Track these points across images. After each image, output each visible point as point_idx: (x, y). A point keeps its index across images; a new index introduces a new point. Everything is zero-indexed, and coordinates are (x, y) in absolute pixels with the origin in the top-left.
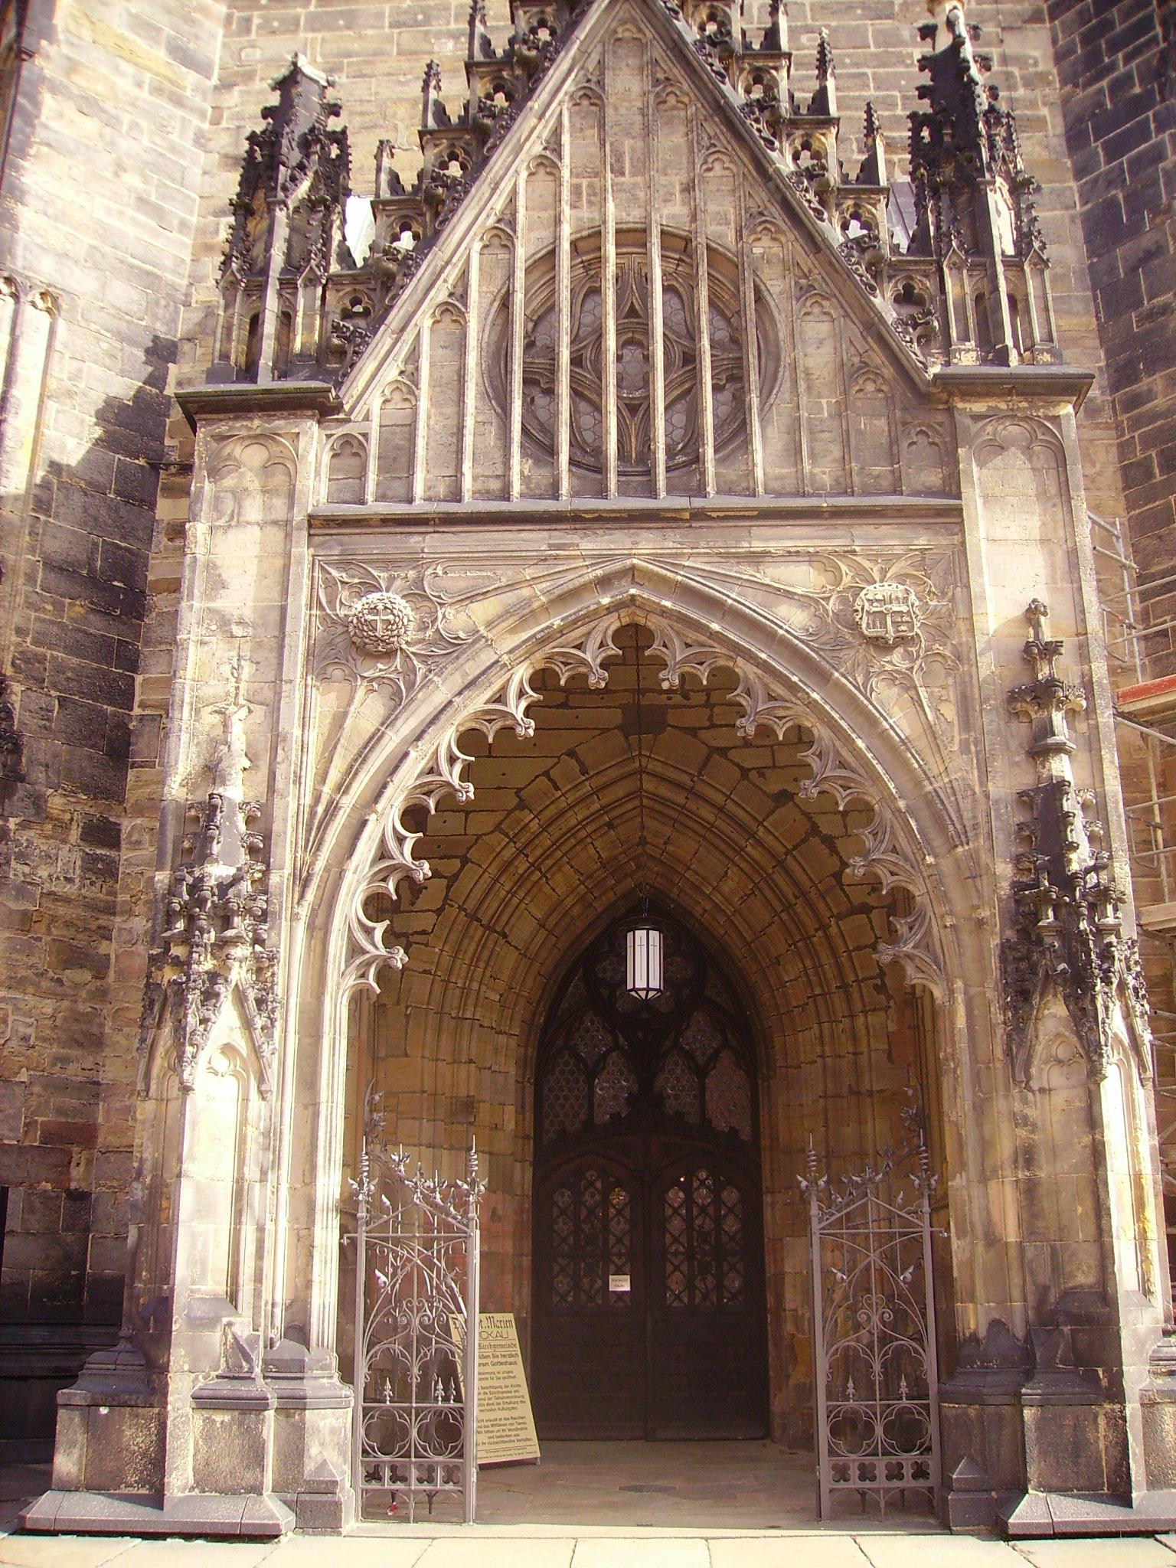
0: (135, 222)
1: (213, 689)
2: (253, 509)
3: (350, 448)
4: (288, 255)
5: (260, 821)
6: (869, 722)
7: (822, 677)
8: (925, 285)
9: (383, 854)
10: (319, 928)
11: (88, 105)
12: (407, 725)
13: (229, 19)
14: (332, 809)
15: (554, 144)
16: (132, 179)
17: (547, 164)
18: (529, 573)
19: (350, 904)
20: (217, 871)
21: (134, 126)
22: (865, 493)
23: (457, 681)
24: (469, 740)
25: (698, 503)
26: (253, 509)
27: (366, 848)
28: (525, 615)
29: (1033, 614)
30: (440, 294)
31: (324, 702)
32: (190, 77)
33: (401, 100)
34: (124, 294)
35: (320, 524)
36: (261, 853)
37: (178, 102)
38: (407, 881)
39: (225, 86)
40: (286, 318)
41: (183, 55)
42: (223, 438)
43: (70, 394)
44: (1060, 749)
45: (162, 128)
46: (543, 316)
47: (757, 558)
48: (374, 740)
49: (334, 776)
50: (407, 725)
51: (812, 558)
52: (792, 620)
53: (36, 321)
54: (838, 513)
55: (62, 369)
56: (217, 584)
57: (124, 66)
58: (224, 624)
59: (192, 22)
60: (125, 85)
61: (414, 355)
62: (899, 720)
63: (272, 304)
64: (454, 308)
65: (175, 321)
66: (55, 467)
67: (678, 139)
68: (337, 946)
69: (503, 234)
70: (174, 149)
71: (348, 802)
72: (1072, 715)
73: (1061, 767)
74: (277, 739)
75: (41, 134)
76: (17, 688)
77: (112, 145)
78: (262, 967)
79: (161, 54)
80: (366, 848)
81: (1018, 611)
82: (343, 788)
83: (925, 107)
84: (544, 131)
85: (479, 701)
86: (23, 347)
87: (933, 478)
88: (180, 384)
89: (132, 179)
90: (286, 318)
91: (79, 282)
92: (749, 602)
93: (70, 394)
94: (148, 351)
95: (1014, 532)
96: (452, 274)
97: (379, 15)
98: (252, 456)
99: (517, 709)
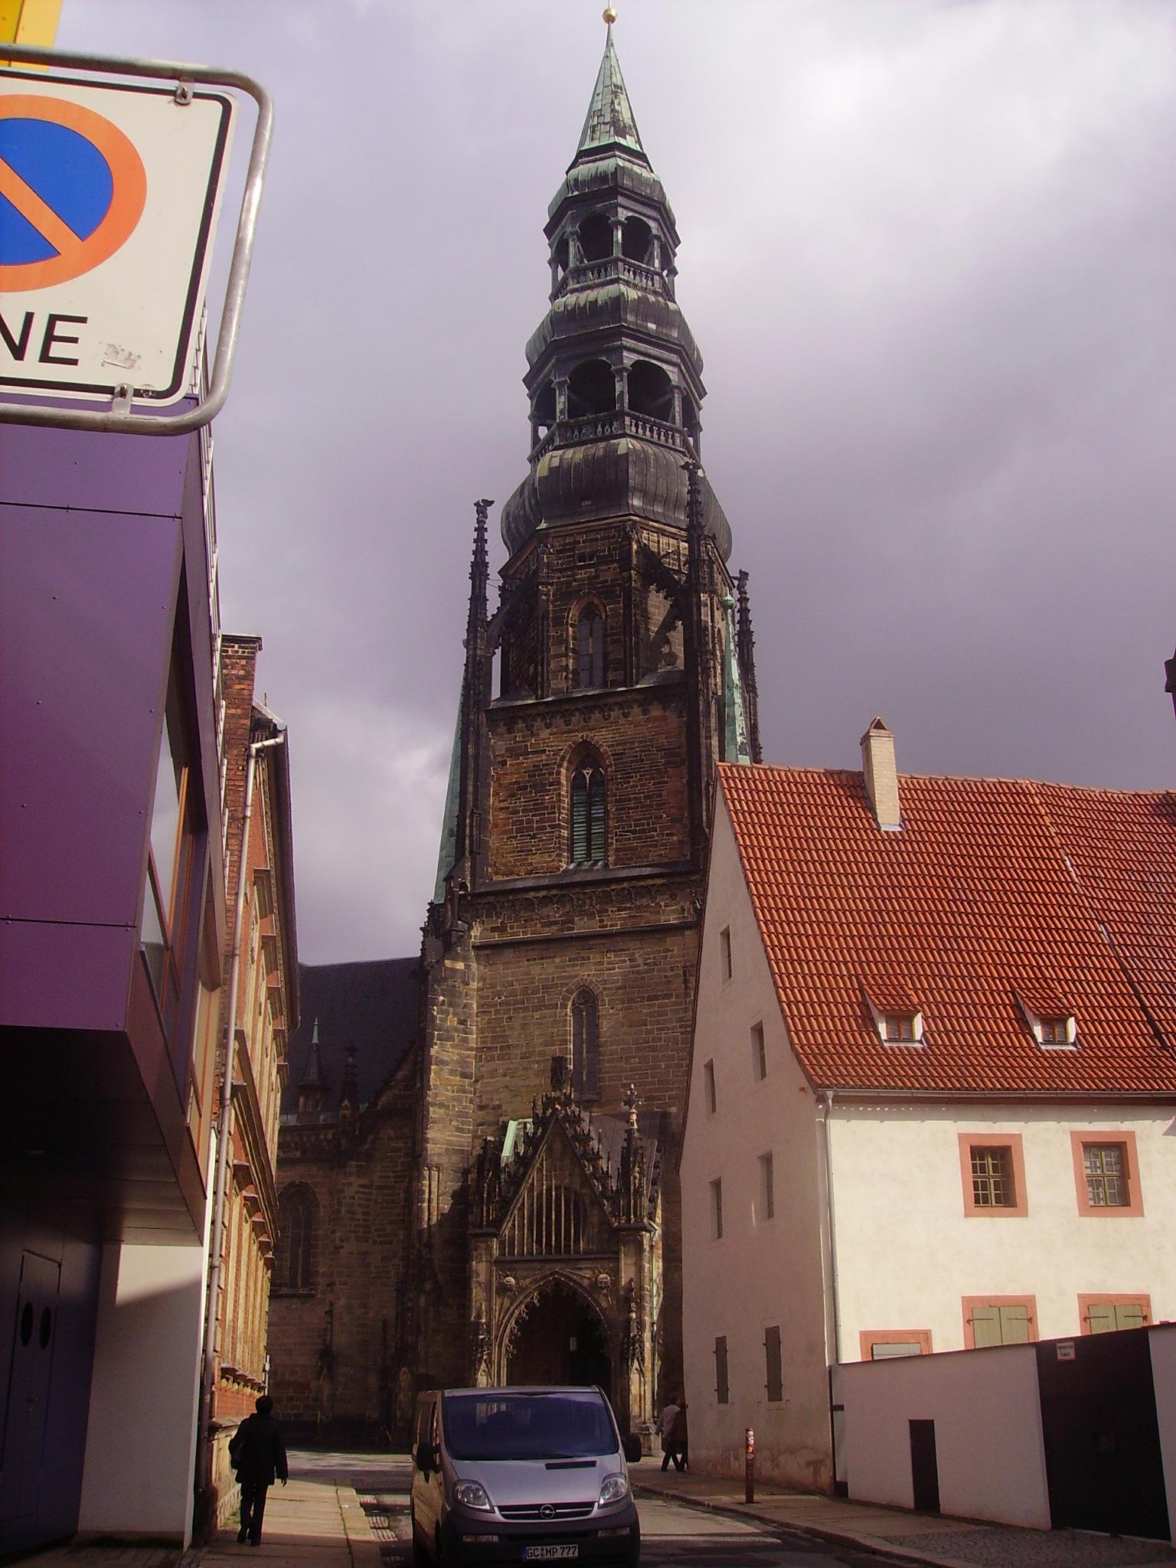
0: (456, 1136)
1: (478, 1298)
2: (484, 1259)
3: (502, 1244)
4: (488, 1194)
5: (489, 1324)
6: (599, 1305)
7: (590, 1295)
8: (617, 1201)
9: (511, 1331)
10: (500, 1347)
11: (441, 1105)
12: (515, 1305)
13: (476, 1055)
14: (502, 1323)
15: (542, 1165)
16: (454, 1123)
17: (540, 1170)
18: (537, 1272)
19: (506, 1341)
20: (481, 1337)
21: (454, 1105)
22: (603, 1253)
23: (524, 1295)
24: (526, 1307)
25: (570, 1257)
26: (484, 1259)
27: (508, 1331)
28: (535, 1281)
29: (631, 1280)
30: (519, 1205)
31: (499, 1301)
32: (467, 1081)
33: (523, 1086)
34: (455, 1158)
35: (497, 1262)
36: (489, 1332)
37: (464, 1091)
38: (515, 1335)
39: (476, 1081)
40: (488, 1211)
41: (464, 1075)
42: (478, 1242)
43: (444, 1193)
44: (632, 1311)
45: (460, 1102)
46: (540, 1207)
47: (580, 1269)
48: (509, 1308)
49: (502, 1315)
50: (515, 1305)
51: (591, 1269)
52: (586, 1282)
53: (435, 1173)
54: (594, 1259)
55: (442, 1188)
56: (478, 1275)
57: (449, 1087)
58: (480, 1283)
59: (466, 1062)
60: (449, 1094)
61: (514, 1221)
62: (604, 1304)
63: (485, 1208)
64: (522, 1208)
65: (468, 1161)
66: (442, 1214)
67: (568, 1161)
68: (503, 1349)
69: (531, 1190)
70: (465, 1107)
71: (504, 1321)
72: (636, 1303)
73: (634, 1315)
74: (491, 1309)
75: (431, 1120)
76: (439, 1275)
77: (448, 1115)
78: (489, 1355)
79: (458, 1078)
80: (508, 1331)
81: (628, 1280)
82: (503, 1318)
83: (626, 1145)
84: (539, 1161)
85: (528, 1300)
86: (433, 1187)
87: (615, 1249)
88: (472, 1180)
89: (454, 1123)
90: (488, 1211)
91: (444, 1160)
92: (578, 1279)
93: (444, 1193)
94: (463, 1173)
95: (630, 1262)
96: (521, 1200)
97: (516, 1054)
98: (483, 1246)
99: (536, 1301)
